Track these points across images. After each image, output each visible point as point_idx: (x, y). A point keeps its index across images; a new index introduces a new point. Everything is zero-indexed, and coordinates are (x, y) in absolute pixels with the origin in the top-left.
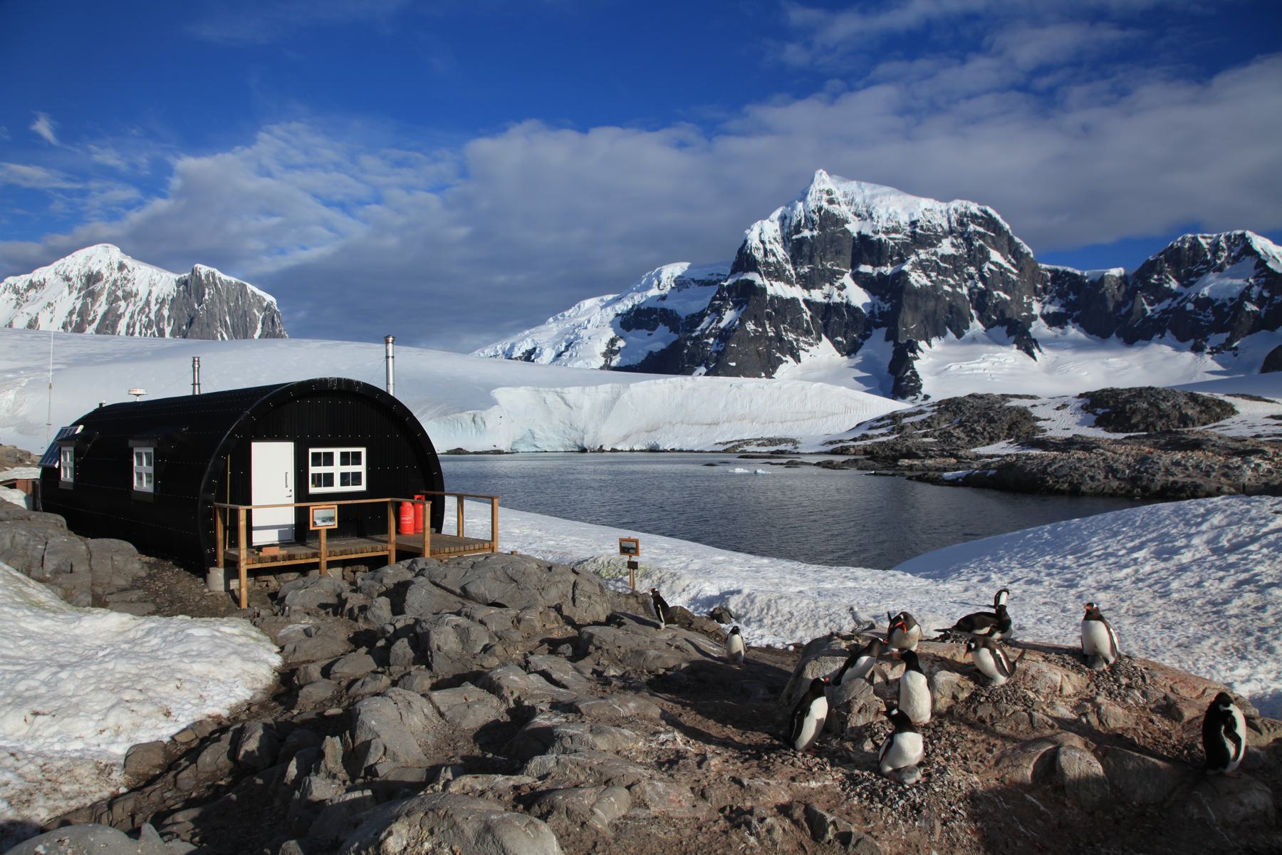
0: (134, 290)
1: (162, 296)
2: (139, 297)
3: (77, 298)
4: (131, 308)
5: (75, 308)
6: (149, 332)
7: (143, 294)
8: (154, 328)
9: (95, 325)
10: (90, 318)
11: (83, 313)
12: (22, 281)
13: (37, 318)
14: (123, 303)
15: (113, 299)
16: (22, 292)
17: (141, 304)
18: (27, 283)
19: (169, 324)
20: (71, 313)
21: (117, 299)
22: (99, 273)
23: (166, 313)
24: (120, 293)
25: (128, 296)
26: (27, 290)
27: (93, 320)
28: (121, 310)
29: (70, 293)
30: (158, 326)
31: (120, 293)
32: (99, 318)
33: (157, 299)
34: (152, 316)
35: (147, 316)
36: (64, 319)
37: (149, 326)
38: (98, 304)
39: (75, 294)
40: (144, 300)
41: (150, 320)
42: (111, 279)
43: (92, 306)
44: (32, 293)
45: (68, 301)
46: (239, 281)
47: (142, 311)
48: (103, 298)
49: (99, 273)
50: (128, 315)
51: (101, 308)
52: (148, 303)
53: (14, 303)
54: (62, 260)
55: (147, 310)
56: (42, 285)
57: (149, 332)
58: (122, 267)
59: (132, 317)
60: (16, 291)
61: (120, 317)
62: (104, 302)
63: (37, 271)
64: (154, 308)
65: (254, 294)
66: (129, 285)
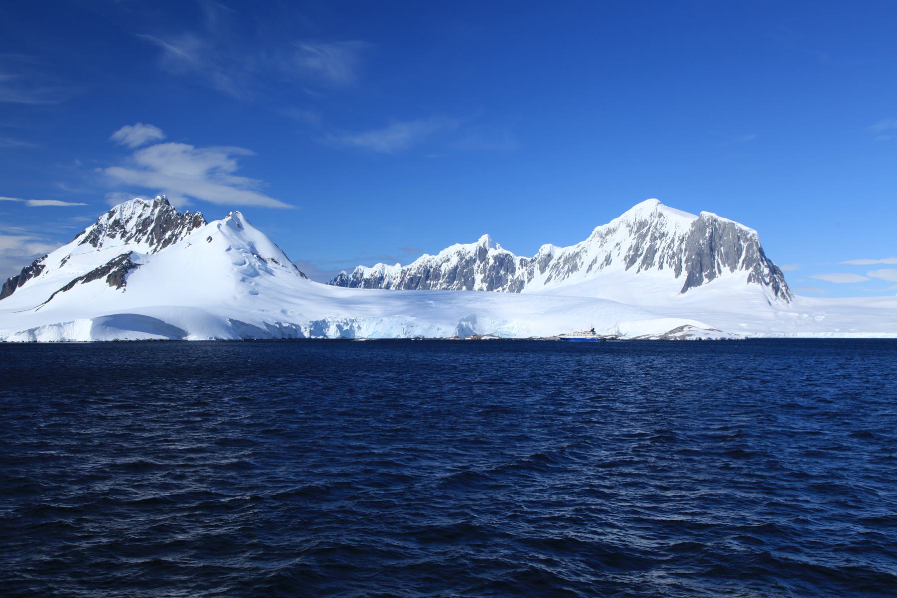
0: (666, 233)
1: (682, 235)
2: (668, 236)
3: (634, 239)
4: (663, 244)
5: (632, 246)
6: (673, 261)
7: (671, 235)
8: (676, 258)
9: (642, 257)
10: (639, 253)
11: (637, 249)
12: (601, 229)
13: (610, 254)
14: (658, 241)
15: (654, 238)
16: (604, 236)
17: (669, 241)
18: (607, 230)
19: (685, 256)
20: (630, 249)
21: (656, 239)
22: (645, 220)
23: (683, 247)
24: (657, 235)
25: (662, 235)
26: (606, 235)
27: (641, 254)
28: (657, 247)
29: (630, 235)
30: (678, 257)
31: (657, 235)
32: (644, 252)
33: (679, 237)
34: (675, 250)
35: (672, 250)
36: (625, 254)
37: (672, 257)
38: (645, 242)
39: (633, 234)
40: (671, 238)
41: (674, 253)
42: (654, 224)
43: (642, 243)
44: (609, 237)
45: (628, 241)
46: (731, 221)
47: (669, 246)
48: (648, 238)
49: (645, 220)
50: (661, 249)
51: (646, 245)
52: (673, 241)
53: (599, 243)
54: (627, 213)
55: (672, 245)
56: (614, 230)
57: (673, 261)
58: (660, 215)
59: (663, 251)
60: (601, 237)
61: (656, 251)
62: (649, 241)
63: (612, 222)
64: (677, 243)
65: (741, 231)
66: (663, 228)
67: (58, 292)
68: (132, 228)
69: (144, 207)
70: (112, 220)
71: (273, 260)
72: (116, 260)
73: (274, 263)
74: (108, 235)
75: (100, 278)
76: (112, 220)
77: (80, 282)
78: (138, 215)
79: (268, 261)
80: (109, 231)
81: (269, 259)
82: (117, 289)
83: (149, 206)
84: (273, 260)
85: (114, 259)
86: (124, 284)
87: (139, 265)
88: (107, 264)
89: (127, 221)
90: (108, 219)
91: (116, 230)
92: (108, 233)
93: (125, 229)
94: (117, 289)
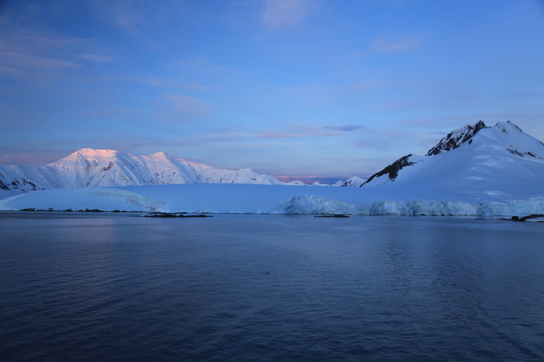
67: (365, 183)
68: (461, 143)
69: (470, 130)
70: (449, 139)
71: (529, 153)
72: (399, 161)
73: (529, 156)
74: (445, 149)
75: (387, 173)
76: (449, 139)
77: (377, 176)
78: (465, 134)
79: (524, 155)
80: (447, 146)
81: (525, 154)
82: (391, 180)
83: (473, 128)
84: (529, 153)
85: (398, 160)
86: (395, 176)
87: (414, 163)
88: (393, 164)
89: (458, 139)
90: (447, 139)
91: (450, 146)
92: (446, 148)
93: (456, 144)
94: (391, 180)
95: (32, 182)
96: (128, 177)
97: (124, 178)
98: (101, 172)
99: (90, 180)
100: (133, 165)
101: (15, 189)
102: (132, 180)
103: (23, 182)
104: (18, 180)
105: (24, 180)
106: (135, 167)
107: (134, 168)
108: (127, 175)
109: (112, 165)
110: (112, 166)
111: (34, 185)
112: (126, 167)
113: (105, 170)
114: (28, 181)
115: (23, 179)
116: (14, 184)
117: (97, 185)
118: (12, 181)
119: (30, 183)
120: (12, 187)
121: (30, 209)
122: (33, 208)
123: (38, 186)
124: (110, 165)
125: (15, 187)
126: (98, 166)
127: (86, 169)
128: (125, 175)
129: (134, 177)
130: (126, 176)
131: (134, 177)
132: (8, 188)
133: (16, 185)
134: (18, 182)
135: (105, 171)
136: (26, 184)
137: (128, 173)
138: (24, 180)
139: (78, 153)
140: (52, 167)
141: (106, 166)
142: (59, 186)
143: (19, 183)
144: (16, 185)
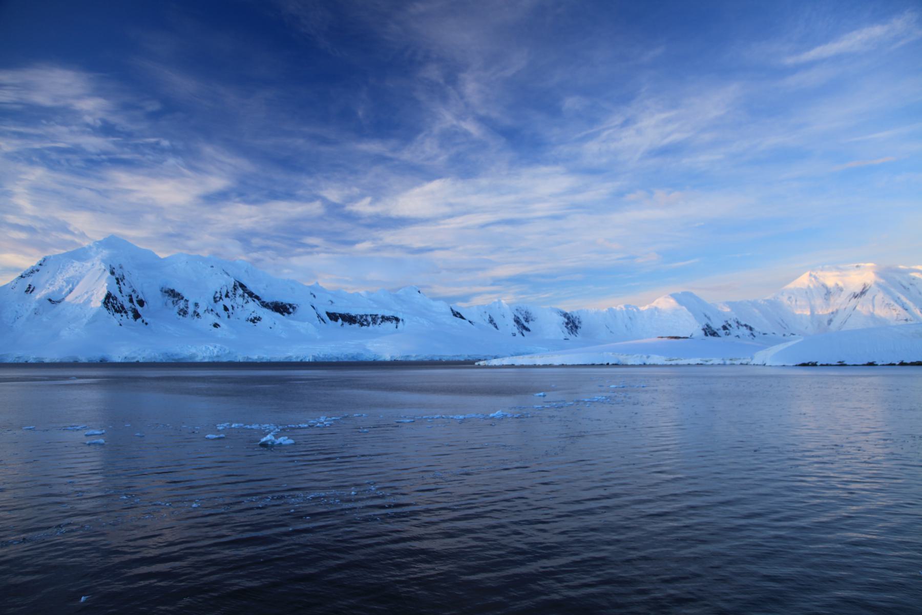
95: (747, 324)
96: (900, 305)
97: (891, 308)
98: (850, 301)
99: (832, 316)
100: (905, 283)
101: (727, 336)
102: (906, 310)
103: (736, 324)
104: (729, 322)
105: (737, 322)
106: (910, 287)
107: (908, 289)
108: (896, 301)
109: (868, 288)
110: (867, 290)
111: (751, 329)
112: (892, 290)
113: (856, 297)
114: (743, 323)
115: (736, 320)
116: (725, 328)
117: (845, 322)
118: (722, 325)
119: (746, 326)
120: (722, 332)
121: (809, 363)
122: (814, 361)
123: (757, 329)
124: (863, 289)
125: (726, 332)
126: (843, 292)
127: (825, 299)
128: (892, 302)
129: (910, 304)
130: (896, 305)
131: (910, 304)
132: (717, 334)
133: (727, 329)
134: (730, 325)
135: (856, 299)
136: (740, 327)
137: (899, 298)
138: (737, 322)
139: (810, 275)
140: (773, 299)
141: (858, 291)
142: (785, 328)
143: (731, 327)
144: (727, 329)
